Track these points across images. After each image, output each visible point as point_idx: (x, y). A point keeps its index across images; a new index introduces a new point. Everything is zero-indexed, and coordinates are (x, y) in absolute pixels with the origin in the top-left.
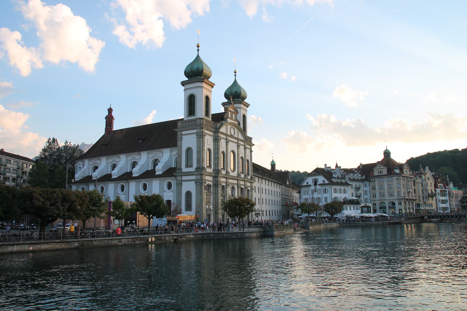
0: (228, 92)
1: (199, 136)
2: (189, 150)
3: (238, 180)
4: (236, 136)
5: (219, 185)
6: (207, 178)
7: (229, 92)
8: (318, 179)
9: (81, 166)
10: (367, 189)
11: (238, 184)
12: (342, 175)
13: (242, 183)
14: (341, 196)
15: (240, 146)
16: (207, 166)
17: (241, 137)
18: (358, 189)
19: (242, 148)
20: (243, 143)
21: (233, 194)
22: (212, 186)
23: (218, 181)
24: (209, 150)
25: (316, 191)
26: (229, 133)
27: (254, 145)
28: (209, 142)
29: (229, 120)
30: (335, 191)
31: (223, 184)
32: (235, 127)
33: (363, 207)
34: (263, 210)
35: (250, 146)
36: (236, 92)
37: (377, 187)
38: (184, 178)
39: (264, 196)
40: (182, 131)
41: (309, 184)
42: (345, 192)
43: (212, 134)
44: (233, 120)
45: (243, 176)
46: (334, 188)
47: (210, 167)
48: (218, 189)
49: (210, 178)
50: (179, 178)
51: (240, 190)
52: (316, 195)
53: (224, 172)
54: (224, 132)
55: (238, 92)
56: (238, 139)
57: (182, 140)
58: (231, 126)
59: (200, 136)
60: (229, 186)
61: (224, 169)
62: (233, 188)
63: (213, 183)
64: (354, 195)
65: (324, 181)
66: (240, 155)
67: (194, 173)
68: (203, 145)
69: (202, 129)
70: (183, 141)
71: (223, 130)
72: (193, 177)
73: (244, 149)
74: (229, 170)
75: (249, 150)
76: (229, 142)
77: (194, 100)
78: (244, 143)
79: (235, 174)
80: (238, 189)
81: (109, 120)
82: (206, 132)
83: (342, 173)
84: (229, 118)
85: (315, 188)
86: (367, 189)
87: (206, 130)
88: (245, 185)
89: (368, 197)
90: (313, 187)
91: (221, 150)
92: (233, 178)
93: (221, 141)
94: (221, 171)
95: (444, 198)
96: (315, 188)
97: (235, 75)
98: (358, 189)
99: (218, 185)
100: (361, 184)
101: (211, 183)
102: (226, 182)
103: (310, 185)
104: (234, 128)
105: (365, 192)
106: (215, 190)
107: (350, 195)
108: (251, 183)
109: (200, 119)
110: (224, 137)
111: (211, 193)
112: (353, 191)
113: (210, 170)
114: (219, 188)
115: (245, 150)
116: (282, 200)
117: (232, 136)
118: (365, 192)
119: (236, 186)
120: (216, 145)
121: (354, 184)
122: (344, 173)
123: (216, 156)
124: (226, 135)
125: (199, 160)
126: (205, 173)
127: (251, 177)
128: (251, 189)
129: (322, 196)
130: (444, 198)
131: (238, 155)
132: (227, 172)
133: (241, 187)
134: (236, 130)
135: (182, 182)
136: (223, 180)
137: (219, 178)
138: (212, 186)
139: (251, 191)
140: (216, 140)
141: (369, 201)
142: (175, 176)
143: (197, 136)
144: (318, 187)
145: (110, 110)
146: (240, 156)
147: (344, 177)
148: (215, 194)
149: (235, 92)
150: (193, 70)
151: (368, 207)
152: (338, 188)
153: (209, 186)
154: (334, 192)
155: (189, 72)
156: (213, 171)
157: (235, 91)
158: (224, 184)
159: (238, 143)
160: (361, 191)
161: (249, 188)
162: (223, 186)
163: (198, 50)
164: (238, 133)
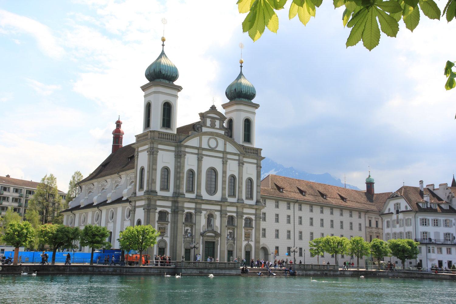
0: (228, 91)
1: (149, 152)
2: (142, 169)
3: (221, 205)
4: (220, 148)
5: (180, 212)
6: (159, 203)
7: (229, 90)
8: (400, 204)
11: (221, 211)
12: (448, 197)
13: (234, 209)
15: (227, 162)
16: (162, 189)
17: (230, 148)
20: (237, 157)
21: (212, 223)
23: (177, 207)
25: (398, 223)
26: (205, 146)
27: (264, 158)
29: (204, 129)
30: (424, 223)
31: (186, 211)
32: (215, 136)
34: (301, 249)
35: (257, 160)
36: (235, 90)
40: (138, 148)
41: (390, 212)
42: (447, 224)
43: (173, 148)
44: (217, 129)
46: (421, 217)
48: (177, 216)
49: (169, 204)
50: (133, 204)
51: (226, 220)
55: (237, 89)
56: (225, 152)
57: (138, 158)
58: (211, 136)
59: (150, 152)
60: (201, 213)
62: (210, 217)
63: (172, 209)
65: (406, 207)
66: (229, 174)
67: (143, 198)
69: (153, 144)
70: (139, 159)
71: (193, 142)
72: (142, 203)
73: (238, 165)
75: (256, 165)
76: (202, 158)
78: (239, 156)
80: (221, 217)
82: (160, 146)
83: (447, 195)
84: (208, 127)
85: (398, 217)
87: (159, 144)
88: (237, 212)
91: (186, 168)
93: (186, 157)
94: (184, 195)
96: (398, 217)
97: (241, 67)
99: (177, 212)
101: (169, 210)
102: (195, 209)
103: (392, 213)
106: (175, 219)
108: (256, 209)
109: (150, 131)
110: (196, 151)
111: (169, 222)
113: (170, 194)
114: (180, 216)
115: (239, 166)
117: (212, 150)
119: (218, 214)
120: (178, 162)
122: (450, 195)
123: (178, 176)
124: (199, 148)
125: (152, 181)
126: (154, 198)
127: (258, 202)
128: (256, 218)
129: (405, 230)
131: (224, 172)
132: (199, 196)
133: (226, 214)
134: (221, 141)
135: (135, 208)
136: (186, 205)
137: (180, 205)
139: (256, 220)
140: (179, 156)
142: (130, 202)
143: (147, 152)
145: (119, 124)
147: (451, 201)
148: (175, 223)
149: (234, 90)
150: (151, 72)
152: (430, 217)
154: (421, 224)
155: (148, 75)
156: (173, 194)
157: (234, 89)
158: (193, 211)
159: (223, 158)
161: (253, 217)
162: (191, 214)
163: (163, 45)
164: (225, 144)
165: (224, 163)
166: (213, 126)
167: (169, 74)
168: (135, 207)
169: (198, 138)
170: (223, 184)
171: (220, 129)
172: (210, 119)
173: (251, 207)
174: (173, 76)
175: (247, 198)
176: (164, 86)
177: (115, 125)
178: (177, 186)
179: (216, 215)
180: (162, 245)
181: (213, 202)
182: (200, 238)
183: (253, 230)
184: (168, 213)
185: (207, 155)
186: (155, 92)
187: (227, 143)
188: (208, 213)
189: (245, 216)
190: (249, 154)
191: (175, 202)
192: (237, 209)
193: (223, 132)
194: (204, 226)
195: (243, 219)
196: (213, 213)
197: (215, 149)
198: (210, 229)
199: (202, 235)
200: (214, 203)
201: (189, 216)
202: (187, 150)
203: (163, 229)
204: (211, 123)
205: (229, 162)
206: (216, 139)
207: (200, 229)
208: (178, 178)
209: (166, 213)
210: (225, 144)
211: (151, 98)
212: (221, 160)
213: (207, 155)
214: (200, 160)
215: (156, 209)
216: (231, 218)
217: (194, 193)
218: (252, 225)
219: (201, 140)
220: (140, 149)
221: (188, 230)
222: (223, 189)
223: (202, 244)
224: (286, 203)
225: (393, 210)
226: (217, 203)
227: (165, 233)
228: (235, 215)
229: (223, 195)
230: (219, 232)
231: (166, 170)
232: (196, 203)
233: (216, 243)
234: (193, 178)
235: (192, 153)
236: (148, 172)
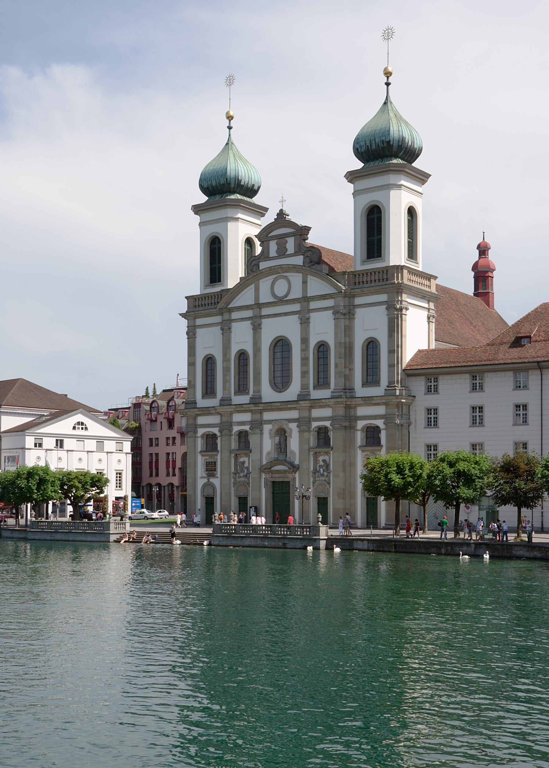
4: (296, 293)
6: (201, 420)
20: (330, 303)
22: (218, 434)
31: (236, 429)
32: (283, 273)
54: (251, 302)
56: (306, 299)
104: (285, 274)
117: (281, 301)
119: (293, 426)
124: (258, 306)
134: (296, 279)
138: (218, 434)
146: (313, 343)
161: (380, 423)
164: (305, 282)
165: (305, 322)
166: (282, 253)
167: (214, 184)
169: (253, 286)
170: (302, 365)
171: (296, 254)
172: (276, 241)
173: (368, 401)
174: (222, 183)
175: (366, 383)
176: (382, 172)
179: (291, 430)
180: (209, 492)
181: (278, 406)
182: (260, 477)
183: (382, 450)
184: (215, 435)
185: (269, 316)
187: (310, 278)
188: (276, 427)
189: (361, 424)
190: (361, 286)
192: (334, 411)
193: (299, 260)
194: (268, 454)
195: (357, 430)
196: (285, 427)
197: (286, 297)
198: (282, 457)
199: (267, 469)
200: (280, 407)
201: (243, 436)
202: (235, 315)
203: (212, 464)
204: (278, 249)
205: (314, 316)
206: (286, 278)
207: (261, 460)
209: (214, 436)
210: (305, 282)
212: (248, 323)
213: (269, 316)
214: (257, 328)
215: (195, 432)
216: (322, 433)
217: (248, 393)
218: (379, 439)
219: (257, 290)
221: (243, 463)
222: (304, 374)
223: (265, 487)
224: (468, 376)
226: (286, 407)
227: (215, 471)
228: (327, 424)
229: (305, 386)
230: (297, 462)
233: (291, 483)
234: (246, 365)
235: (243, 319)
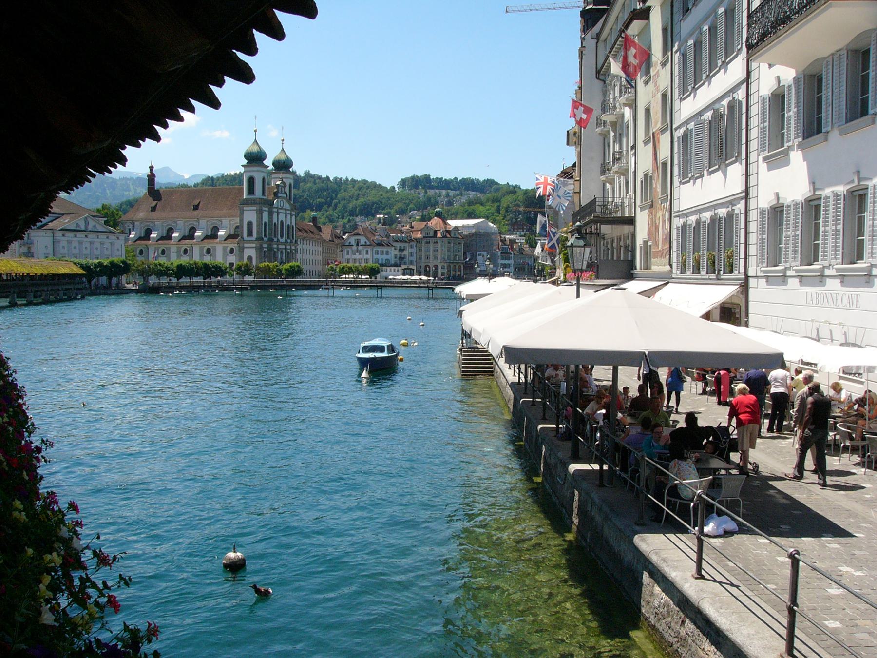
2: (250, 224)
9: (131, 227)
10: (414, 250)
14: (382, 258)
17: (288, 207)
18: (401, 250)
19: (289, 216)
24: (265, 223)
28: (265, 217)
29: (279, 195)
30: (377, 253)
33: (405, 269)
37: (423, 248)
38: (246, 245)
39: (305, 256)
42: (387, 253)
43: (267, 209)
45: (289, 241)
47: (265, 236)
52: (357, 256)
53: (275, 240)
56: (286, 209)
61: (275, 236)
62: (282, 252)
64: (398, 256)
68: (262, 219)
72: (254, 245)
74: (279, 238)
77: (253, 182)
79: (283, 240)
81: (151, 177)
82: (264, 208)
86: (414, 250)
89: (414, 259)
90: (355, 248)
92: (282, 243)
95: (506, 262)
98: (401, 250)
100: (406, 245)
105: (411, 254)
107: (393, 255)
112: (397, 252)
113: (266, 239)
116: (323, 259)
117: (282, 208)
118: (411, 254)
121: (398, 245)
124: (278, 208)
130: (506, 262)
132: (278, 240)
136: (275, 246)
140: (271, 214)
141: (415, 263)
144: (360, 248)
145: (151, 168)
151: (411, 269)
152: (380, 249)
153: (265, 252)
160: (406, 253)
168: (243, 248)
177: (149, 170)
178: (270, 234)
186: (258, 171)
191: (268, 245)
208: (270, 229)
211: (254, 175)
220: (245, 208)
225: (353, 243)
231: (265, 223)
232: (278, 245)
236: (257, 226)
